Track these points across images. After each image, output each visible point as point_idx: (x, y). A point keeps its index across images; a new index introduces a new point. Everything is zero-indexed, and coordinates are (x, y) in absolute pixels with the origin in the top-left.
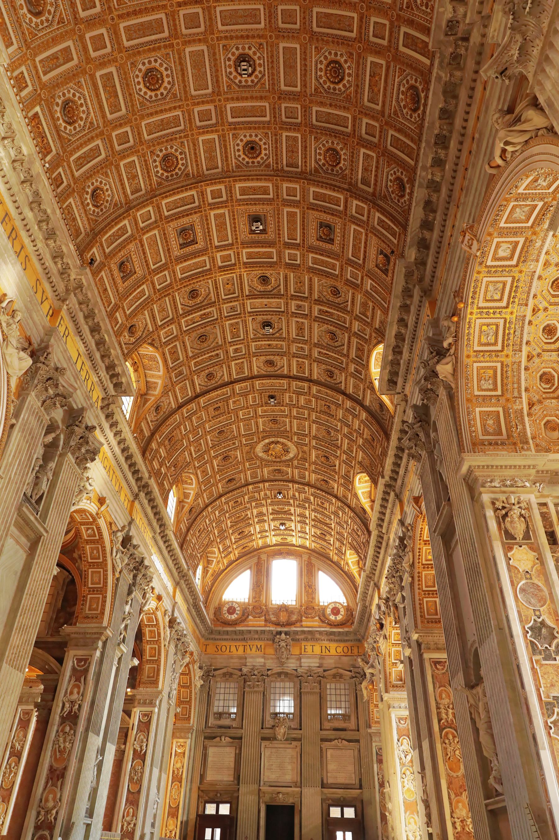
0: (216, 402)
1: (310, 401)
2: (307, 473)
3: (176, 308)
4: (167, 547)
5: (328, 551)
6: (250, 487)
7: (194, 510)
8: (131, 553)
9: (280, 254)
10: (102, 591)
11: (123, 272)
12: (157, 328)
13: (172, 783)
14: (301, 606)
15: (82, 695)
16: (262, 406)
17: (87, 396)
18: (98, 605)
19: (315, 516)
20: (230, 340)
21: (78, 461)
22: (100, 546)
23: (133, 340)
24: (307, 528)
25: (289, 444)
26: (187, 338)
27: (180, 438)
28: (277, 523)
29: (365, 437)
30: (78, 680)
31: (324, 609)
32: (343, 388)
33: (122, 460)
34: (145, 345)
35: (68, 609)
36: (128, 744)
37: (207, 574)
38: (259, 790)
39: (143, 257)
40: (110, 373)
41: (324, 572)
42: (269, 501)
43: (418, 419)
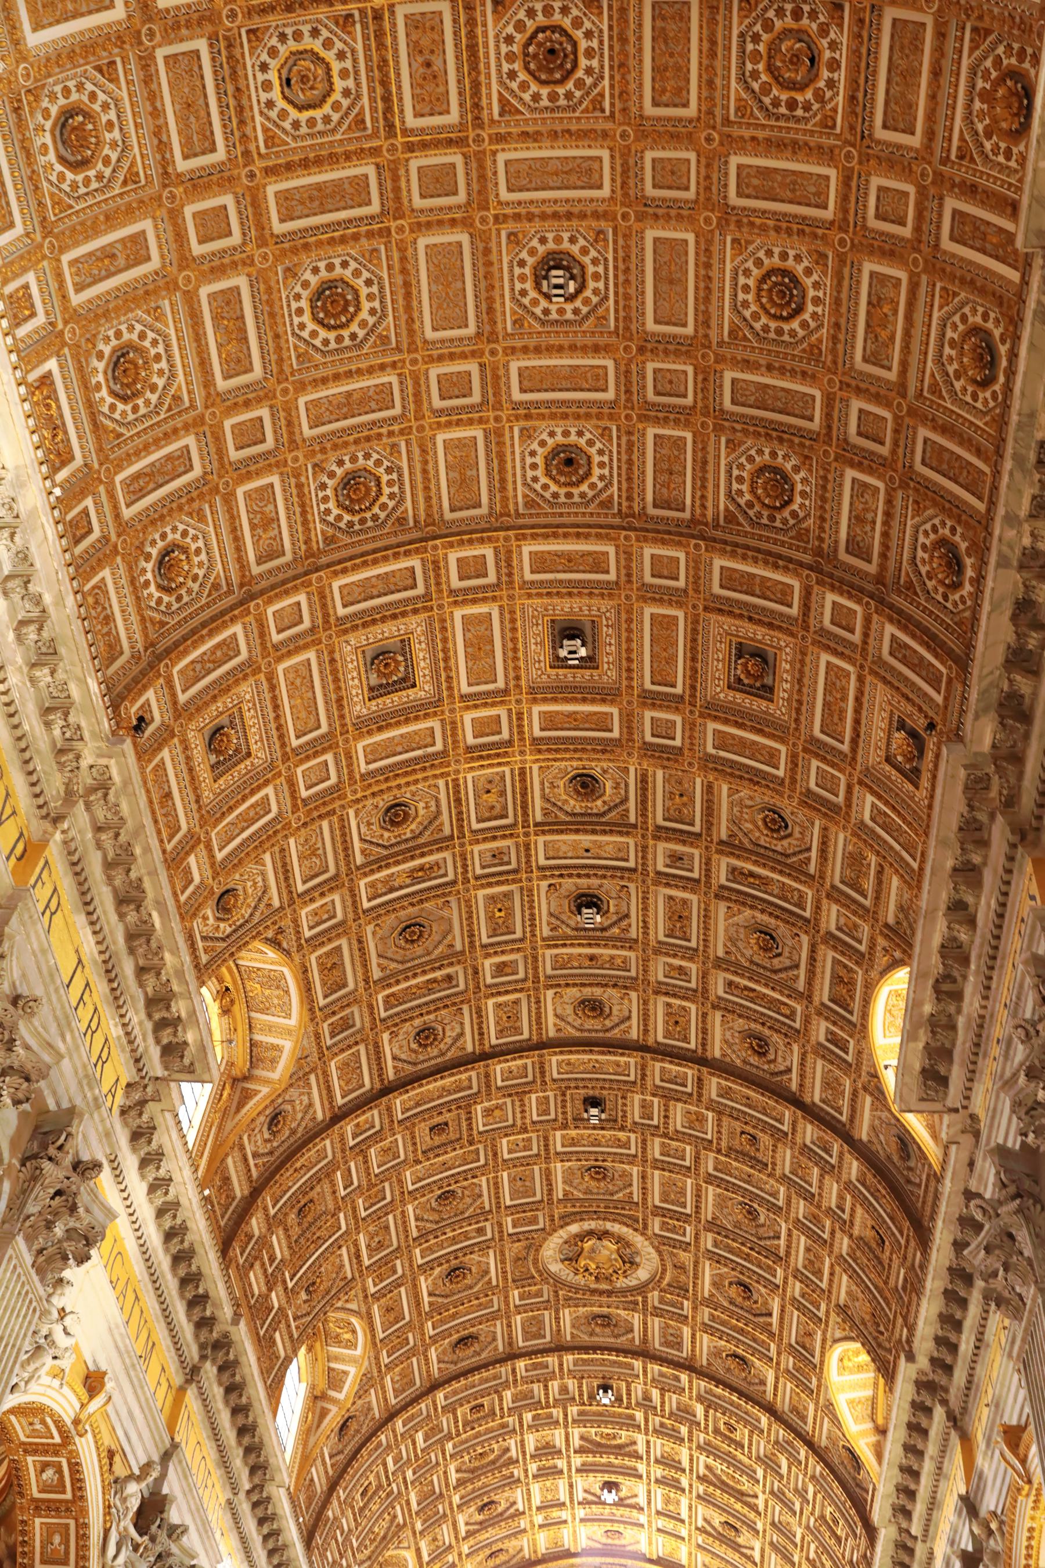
0: (438, 1110)
1: (701, 1119)
2: (687, 1331)
3: (347, 848)
4: (266, 1538)
6: (521, 1364)
7: (353, 1426)
8: (159, 1549)
9: (629, 721)
11: (218, 752)
12: (293, 899)
16: (565, 1126)
17: (87, 1076)
19: (708, 1467)
20: (485, 940)
21: (41, 1259)
22: (72, 1523)
23: (225, 928)
24: (684, 1502)
25: (638, 1240)
26: (370, 929)
27: (331, 1206)
28: (594, 1481)
29: (856, 1232)
32: (794, 1086)
33: (163, 1261)
34: (257, 944)
39: (272, 715)
40: (157, 1016)
42: (573, 1410)
43: (1012, 1189)
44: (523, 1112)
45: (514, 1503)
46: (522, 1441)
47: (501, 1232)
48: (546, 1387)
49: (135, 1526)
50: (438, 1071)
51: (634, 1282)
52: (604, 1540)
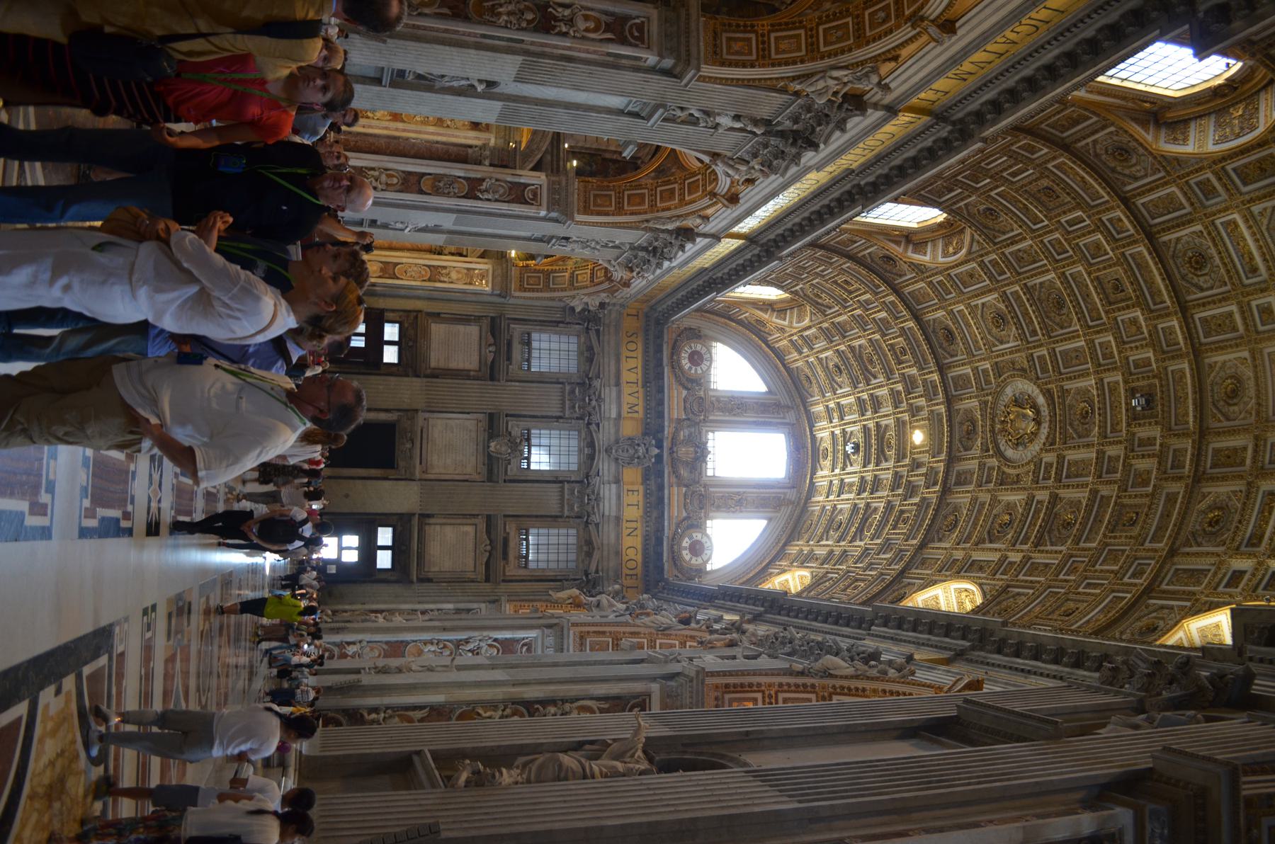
5: (806, 536)
6: (935, 377)
10: (764, 58)
13: (429, 266)
14: (705, 486)
15: (583, 38)
16: (1126, 382)
18: (737, 53)
19: (876, 509)
24: (852, 496)
25: (1035, 447)
28: (859, 438)
30: (608, 28)
31: (700, 527)
35: (725, 9)
36: (491, 169)
37: (761, 310)
38: (417, 411)
41: (765, 530)
42: (906, 417)
44: (1137, 347)
45: (841, 388)
46: (882, 386)
47: (1035, 347)
48: (922, 396)
49: (845, 94)
50: (1168, 276)
51: (1002, 448)
52: (821, 448)
